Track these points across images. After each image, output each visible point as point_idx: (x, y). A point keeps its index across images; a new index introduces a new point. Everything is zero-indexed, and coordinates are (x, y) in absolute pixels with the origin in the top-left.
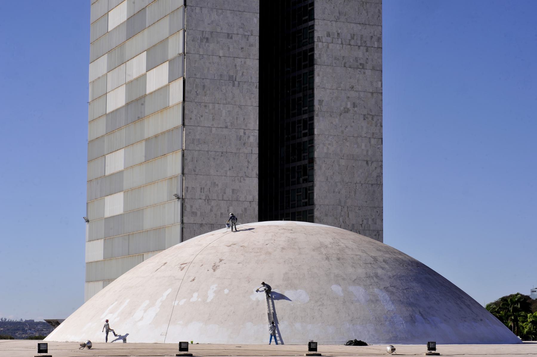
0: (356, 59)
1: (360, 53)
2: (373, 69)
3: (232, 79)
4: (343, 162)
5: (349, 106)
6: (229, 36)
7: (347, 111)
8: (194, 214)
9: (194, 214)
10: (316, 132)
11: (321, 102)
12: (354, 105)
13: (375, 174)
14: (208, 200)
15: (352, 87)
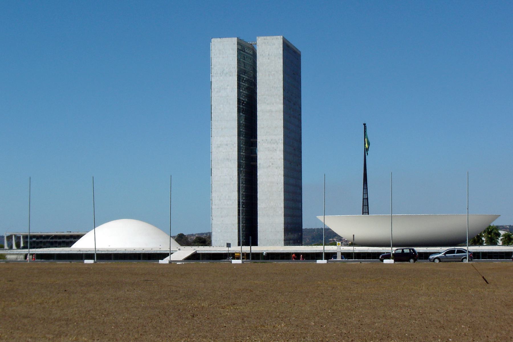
0: (273, 148)
1: (274, 146)
2: (280, 150)
3: (228, 159)
4: (268, 184)
5: (271, 164)
6: (227, 145)
7: (269, 166)
8: (215, 205)
9: (215, 205)
10: (258, 174)
11: (260, 164)
12: (272, 164)
13: (280, 188)
14: (220, 200)
15: (272, 158)
